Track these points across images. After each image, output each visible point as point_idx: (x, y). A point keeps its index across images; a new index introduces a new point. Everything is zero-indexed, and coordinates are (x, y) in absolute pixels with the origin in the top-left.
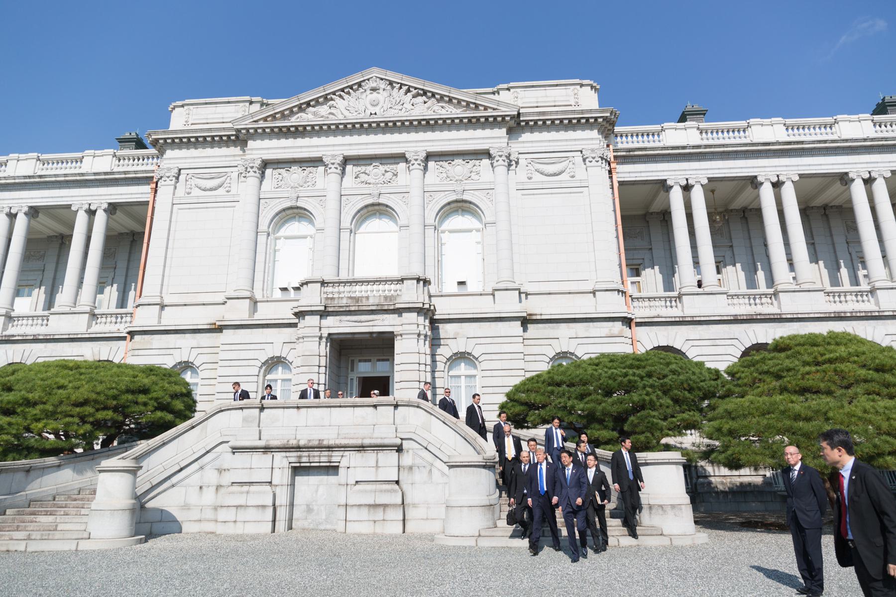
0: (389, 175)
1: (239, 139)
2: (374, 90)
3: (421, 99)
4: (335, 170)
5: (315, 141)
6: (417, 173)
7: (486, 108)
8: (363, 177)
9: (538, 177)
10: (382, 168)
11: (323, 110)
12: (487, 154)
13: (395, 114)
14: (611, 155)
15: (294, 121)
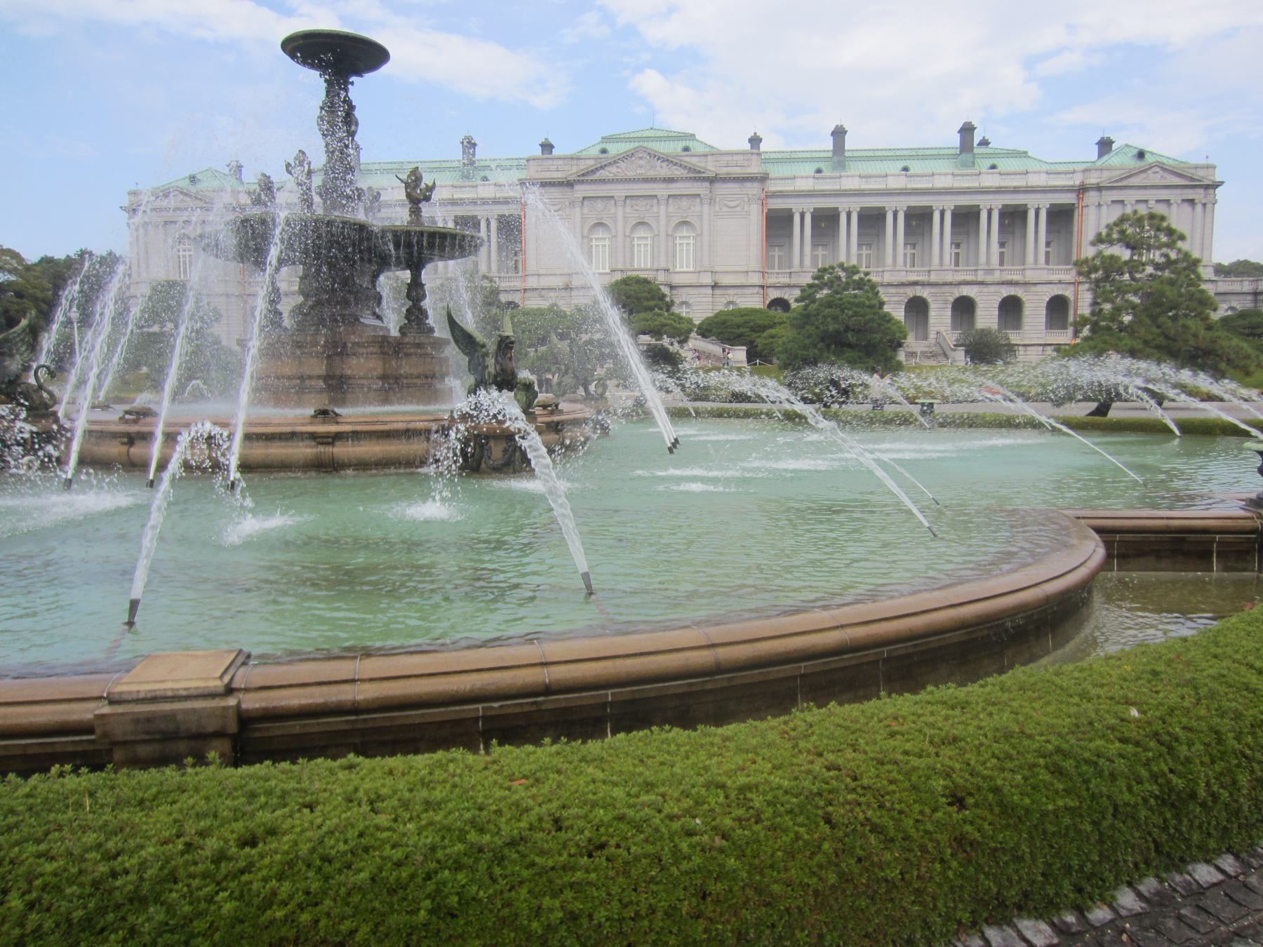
0: (648, 207)
1: (569, 184)
2: (641, 158)
3: (665, 164)
4: (620, 203)
5: (610, 186)
6: (663, 208)
7: (699, 172)
8: (635, 207)
9: (725, 209)
10: (645, 202)
11: (613, 169)
12: (699, 195)
13: (651, 174)
14: (763, 196)
15: (597, 176)
